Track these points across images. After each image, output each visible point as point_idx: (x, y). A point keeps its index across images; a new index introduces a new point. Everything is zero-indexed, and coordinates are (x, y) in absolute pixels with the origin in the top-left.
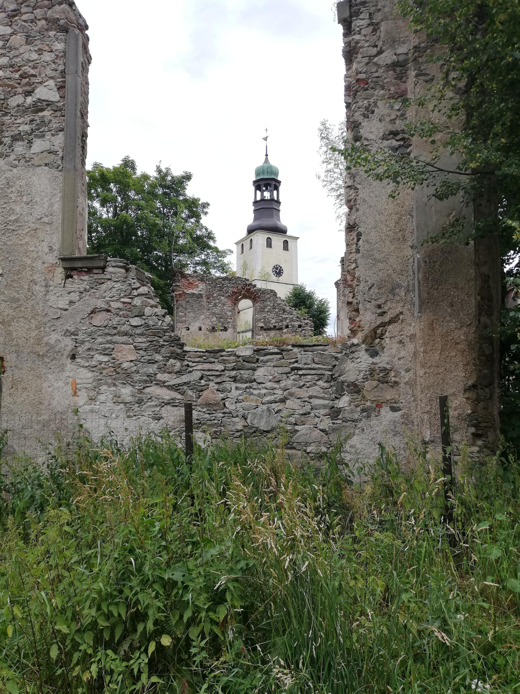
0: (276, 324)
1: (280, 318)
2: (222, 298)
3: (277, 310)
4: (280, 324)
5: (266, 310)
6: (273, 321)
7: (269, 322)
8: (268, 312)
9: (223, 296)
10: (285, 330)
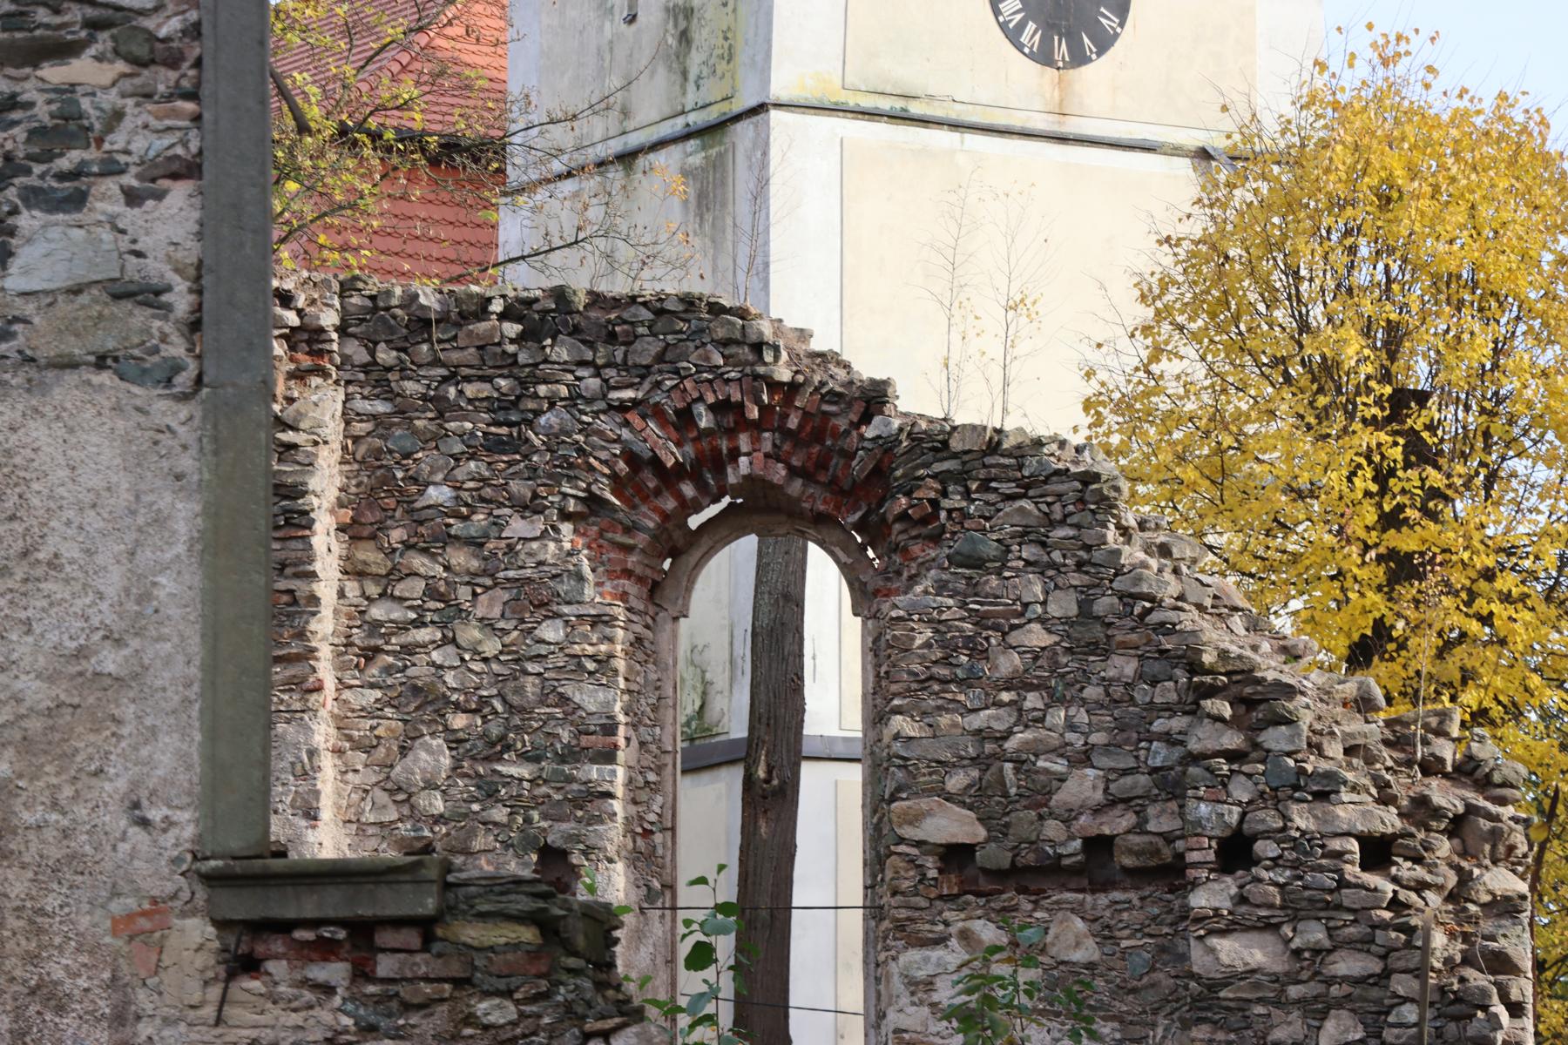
0: (1118, 823)
1: (1160, 755)
2: (518, 527)
3: (1124, 666)
4: (1161, 820)
5: (1009, 663)
6: (1083, 786)
7: (1039, 795)
8: (1018, 683)
9: (529, 507)
10: (1213, 895)
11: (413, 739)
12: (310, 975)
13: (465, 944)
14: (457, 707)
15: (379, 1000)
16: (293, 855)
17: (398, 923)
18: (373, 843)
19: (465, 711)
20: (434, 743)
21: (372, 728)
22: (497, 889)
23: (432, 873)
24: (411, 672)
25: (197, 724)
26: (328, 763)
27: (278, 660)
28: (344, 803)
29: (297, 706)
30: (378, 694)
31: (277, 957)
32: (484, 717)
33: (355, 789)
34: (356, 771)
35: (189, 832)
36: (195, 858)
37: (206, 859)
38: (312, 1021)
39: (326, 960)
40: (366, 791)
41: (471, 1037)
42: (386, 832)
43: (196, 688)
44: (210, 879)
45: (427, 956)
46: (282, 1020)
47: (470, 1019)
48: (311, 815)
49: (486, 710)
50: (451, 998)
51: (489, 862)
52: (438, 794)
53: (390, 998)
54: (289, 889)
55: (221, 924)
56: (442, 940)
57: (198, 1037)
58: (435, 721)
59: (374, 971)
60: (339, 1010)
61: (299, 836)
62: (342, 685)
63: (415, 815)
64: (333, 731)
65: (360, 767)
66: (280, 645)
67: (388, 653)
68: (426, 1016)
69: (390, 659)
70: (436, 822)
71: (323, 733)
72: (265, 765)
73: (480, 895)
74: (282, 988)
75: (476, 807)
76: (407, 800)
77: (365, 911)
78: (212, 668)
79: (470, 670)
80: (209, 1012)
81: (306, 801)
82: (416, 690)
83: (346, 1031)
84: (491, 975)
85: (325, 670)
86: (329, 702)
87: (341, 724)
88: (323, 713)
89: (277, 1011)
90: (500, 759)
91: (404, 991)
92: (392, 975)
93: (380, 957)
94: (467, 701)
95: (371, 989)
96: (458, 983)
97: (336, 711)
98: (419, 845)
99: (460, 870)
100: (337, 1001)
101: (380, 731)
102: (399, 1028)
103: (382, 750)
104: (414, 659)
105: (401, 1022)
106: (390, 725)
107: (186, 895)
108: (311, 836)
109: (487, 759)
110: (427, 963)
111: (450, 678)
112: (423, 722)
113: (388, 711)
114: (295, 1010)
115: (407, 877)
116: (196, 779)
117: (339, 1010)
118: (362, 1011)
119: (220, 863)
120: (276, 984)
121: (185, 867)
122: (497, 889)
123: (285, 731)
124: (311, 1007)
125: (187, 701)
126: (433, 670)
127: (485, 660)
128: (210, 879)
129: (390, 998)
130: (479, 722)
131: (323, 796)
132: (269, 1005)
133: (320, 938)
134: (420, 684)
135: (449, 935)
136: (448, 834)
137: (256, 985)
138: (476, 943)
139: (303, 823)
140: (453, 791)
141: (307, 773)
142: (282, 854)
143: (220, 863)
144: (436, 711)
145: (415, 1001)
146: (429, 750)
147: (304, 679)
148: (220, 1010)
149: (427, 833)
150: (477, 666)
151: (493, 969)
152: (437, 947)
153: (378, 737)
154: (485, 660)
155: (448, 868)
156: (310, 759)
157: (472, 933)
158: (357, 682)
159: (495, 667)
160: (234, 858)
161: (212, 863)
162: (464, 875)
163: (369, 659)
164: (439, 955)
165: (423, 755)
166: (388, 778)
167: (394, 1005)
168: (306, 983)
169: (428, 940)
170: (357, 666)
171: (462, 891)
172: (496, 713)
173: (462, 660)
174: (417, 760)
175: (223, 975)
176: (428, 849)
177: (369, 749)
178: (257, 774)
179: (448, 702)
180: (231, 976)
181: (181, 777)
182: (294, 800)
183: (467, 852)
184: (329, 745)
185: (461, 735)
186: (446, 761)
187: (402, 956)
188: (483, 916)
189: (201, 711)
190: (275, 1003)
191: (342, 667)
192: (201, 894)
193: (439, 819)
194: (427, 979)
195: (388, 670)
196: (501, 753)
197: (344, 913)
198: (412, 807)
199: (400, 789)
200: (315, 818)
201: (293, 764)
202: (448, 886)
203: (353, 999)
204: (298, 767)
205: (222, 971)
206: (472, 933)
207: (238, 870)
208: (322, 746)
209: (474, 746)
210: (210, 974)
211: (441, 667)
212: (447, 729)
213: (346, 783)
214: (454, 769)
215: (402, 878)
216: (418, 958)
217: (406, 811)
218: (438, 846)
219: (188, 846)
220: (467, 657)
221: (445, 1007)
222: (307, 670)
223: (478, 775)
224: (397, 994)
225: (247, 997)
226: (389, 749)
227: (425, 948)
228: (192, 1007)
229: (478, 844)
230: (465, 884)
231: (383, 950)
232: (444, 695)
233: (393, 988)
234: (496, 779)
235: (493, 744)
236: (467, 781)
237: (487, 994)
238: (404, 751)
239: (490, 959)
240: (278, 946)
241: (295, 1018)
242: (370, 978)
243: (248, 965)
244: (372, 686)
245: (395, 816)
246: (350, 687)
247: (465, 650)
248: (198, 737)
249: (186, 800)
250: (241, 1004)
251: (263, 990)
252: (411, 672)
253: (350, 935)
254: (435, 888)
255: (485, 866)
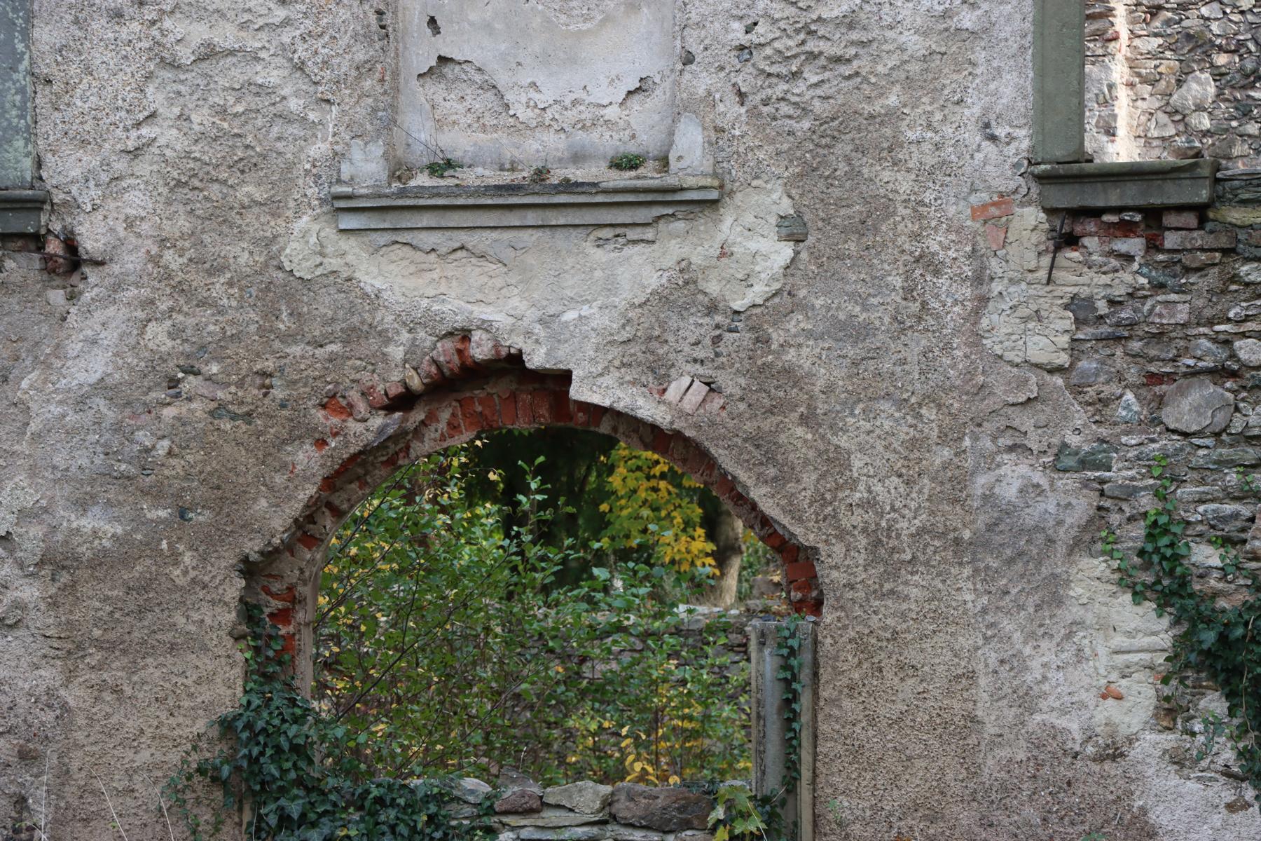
11: (1187, 74)
12: (1115, 248)
13: (1230, 224)
14: (1221, 49)
15: (1167, 265)
16: (1097, 161)
17: (1180, 209)
18: (1156, 152)
19: (1227, 52)
20: (1203, 76)
21: (1156, 67)
22: (1255, 182)
23: (1206, 172)
24: (1185, 23)
25: (1030, 65)
26: (1123, 94)
27: (1089, 17)
28: (1135, 123)
29: (1100, 52)
30: (1160, 41)
31: (1090, 235)
32: (1241, 56)
33: (1144, 112)
34: (1144, 99)
35: (1025, 144)
36: (1030, 162)
37: (1039, 164)
38: (1117, 281)
39: (1126, 236)
40: (1151, 114)
41: (1236, 291)
42: (1167, 144)
43: (1029, 38)
44: (1041, 179)
45: (1202, 232)
46: (1095, 280)
47: (1235, 279)
48: (1111, 132)
49: (1243, 51)
50: (1220, 263)
51: (1244, 164)
52: (1205, 115)
53: (1175, 263)
54: (1099, 185)
55: (1050, 212)
56: (1213, 221)
57: (1035, 292)
58: (1203, 60)
59: (1162, 244)
60: (1137, 272)
61: (1102, 149)
62: (1134, 35)
63: (1188, 130)
64: (1126, 70)
65: (1146, 96)
66: (1089, 6)
67: (1167, 10)
68: (1201, 277)
69: (1169, 14)
70: (1204, 136)
71: (1119, 71)
72: (1081, 92)
73: (1242, 187)
74: (1095, 257)
75: (1234, 124)
76: (1183, 120)
77: (1156, 200)
78: (1040, 24)
79: (1231, 21)
80: (1042, 274)
81: (1107, 122)
82: (1189, 37)
83: (1143, 288)
84: (1250, 246)
85: (1121, 24)
86: (1124, 49)
87: (1132, 64)
88: (1119, 57)
89: (1092, 274)
90: (1253, 87)
91: (1186, 259)
92: (1176, 247)
93: (1167, 233)
94: (1228, 44)
95: (1161, 257)
96: (1225, 252)
97: (1129, 55)
98: (1191, 153)
99: (1227, 169)
100: (1136, 266)
101: (1161, 69)
102: (1181, 286)
103: (1163, 83)
104: (1188, 13)
105: (1183, 281)
106: (1169, 64)
107: (1024, 191)
108: (1111, 148)
109: (1243, 87)
110: (1202, 238)
111: (1215, 27)
112: (1194, 61)
113: (1168, 54)
114: (1104, 273)
115: (1187, 175)
116: (1030, 106)
117: (1137, 272)
118: (1154, 273)
119: (1048, 167)
120: (1090, 254)
121: (1022, 170)
122: (1255, 182)
123: (1091, 71)
124: (1117, 271)
125: (1022, 48)
126: (1202, 21)
127: (1242, 12)
128: (1041, 179)
129: (1175, 263)
130: (1237, 59)
131: (1119, 119)
132: (1086, 269)
133: (1122, 220)
134: (1192, 32)
135: (1219, 217)
136: (1213, 145)
137: (1075, 255)
138: (1239, 223)
139: (1105, 138)
140: (1216, 112)
141: (1107, 101)
142: (1091, 161)
143: (1048, 167)
144: (1204, 53)
145: (1194, 265)
146: (1199, 82)
147: (1105, 31)
148: (1050, 273)
149: (1197, 144)
150: (1236, 18)
151: (1253, 241)
152: (1209, 226)
153: (1160, 74)
154: (1242, 12)
155: (1218, 168)
156: (1110, 91)
157: (1236, 215)
158: (1145, 33)
159: (1250, 17)
160: (1058, 163)
161: (1043, 167)
162: (1229, 173)
163: (1153, 15)
164: (1211, 232)
165: (1194, 86)
166: (1168, 103)
167: (1178, 268)
168: (1112, 253)
169: (1202, 221)
170: (1144, 20)
171: (1228, 185)
172: (1250, 52)
173: (1225, 13)
174: (1189, 90)
175: (1052, 248)
176: (1198, 154)
177: (1153, 83)
178: (1075, 101)
179: (1213, 45)
180: (1058, 248)
181: (1019, 104)
182: (1098, 122)
183: (1229, 158)
184: (1124, 81)
185: (1223, 70)
186: (1212, 90)
187: (1183, 233)
188: (1244, 202)
189: (1033, 55)
190: (1090, 268)
191: (1133, 22)
192: (1035, 190)
193: (1206, 133)
194: (1202, 250)
195: (1168, 23)
196: (1254, 82)
197: (1140, 202)
198: (1186, 125)
199: (1177, 112)
200: (1114, 135)
201: (1097, 95)
202: (1217, 181)
203: (1147, 264)
204: (1101, 97)
205: (1051, 244)
206: (1236, 215)
207: (1061, 172)
208: (1118, 81)
209: (1233, 78)
210: (1042, 247)
211: (1208, 19)
212: (1212, 66)
213: (1137, 108)
214: (1218, 96)
215: (1182, 176)
216: (1195, 234)
217: (1181, 128)
218: (1206, 153)
219: (1025, 154)
220: (1228, 11)
221: (1216, 270)
222: (1108, 25)
223: (1236, 99)
224: (1180, 261)
225: (1069, 264)
226: (1168, 82)
227: (1201, 226)
228: (1030, 271)
229: (1236, 151)
230: (1231, 179)
231: (1169, 229)
232: (1210, 40)
233: (1177, 257)
234: (1250, 102)
235: (1248, 76)
236: (1227, 104)
237: (1248, 260)
238: (1180, 83)
239: (1250, 235)
240: (1091, 226)
241: (1105, 279)
242: (1160, 249)
243: (1071, 241)
244: (1156, 35)
245: (1173, 132)
246: (1140, 36)
247: (1227, 5)
248: (1031, 75)
249: (1023, 121)
250: (1066, 269)
251: (1081, 259)
252: (1185, 23)
253: (1144, 218)
254: (1207, 182)
255: (1240, 167)
